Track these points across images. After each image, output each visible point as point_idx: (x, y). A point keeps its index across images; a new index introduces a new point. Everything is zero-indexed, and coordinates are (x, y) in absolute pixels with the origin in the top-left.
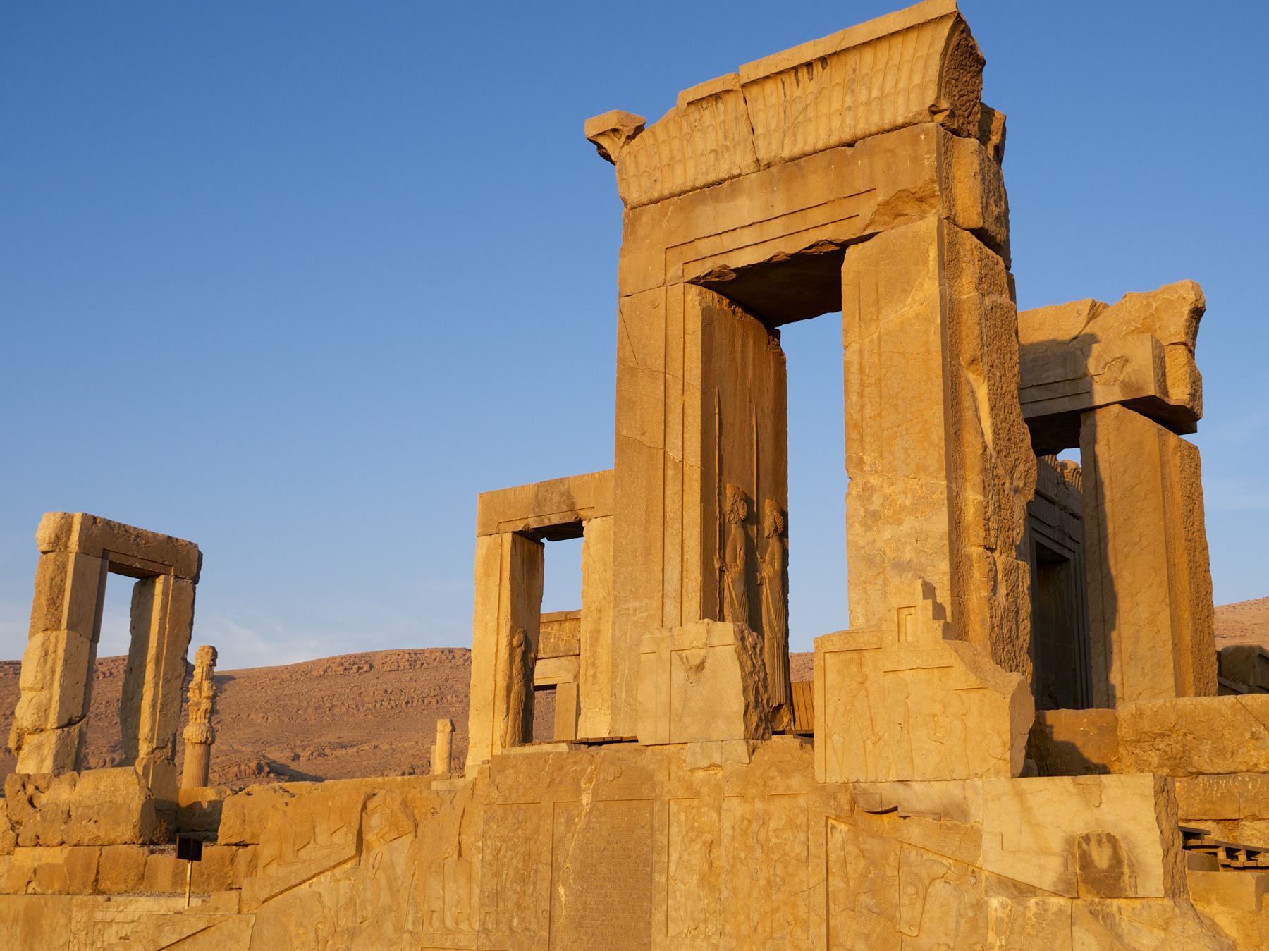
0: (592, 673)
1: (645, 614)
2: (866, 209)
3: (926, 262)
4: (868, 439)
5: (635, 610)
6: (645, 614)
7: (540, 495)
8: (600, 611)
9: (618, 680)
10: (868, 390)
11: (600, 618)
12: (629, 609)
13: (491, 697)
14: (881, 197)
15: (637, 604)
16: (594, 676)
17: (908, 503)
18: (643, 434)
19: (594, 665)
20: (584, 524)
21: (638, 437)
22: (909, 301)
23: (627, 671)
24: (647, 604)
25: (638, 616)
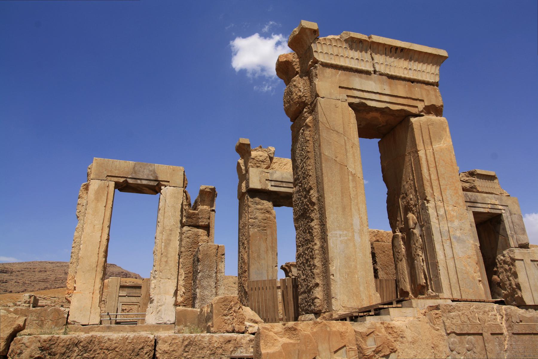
0: (165, 260)
1: (346, 238)
2: (421, 106)
3: (446, 132)
4: (434, 187)
5: (340, 235)
6: (346, 238)
7: (136, 168)
8: (171, 230)
9: (334, 268)
10: (431, 169)
11: (171, 234)
12: (337, 234)
13: (94, 266)
14: (426, 104)
15: (341, 233)
16: (166, 262)
17: (455, 214)
18: (336, 157)
19: (166, 256)
20: (162, 187)
21: (334, 158)
22: (442, 142)
23: (339, 264)
24: (346, 234)
25: (342, 238)
